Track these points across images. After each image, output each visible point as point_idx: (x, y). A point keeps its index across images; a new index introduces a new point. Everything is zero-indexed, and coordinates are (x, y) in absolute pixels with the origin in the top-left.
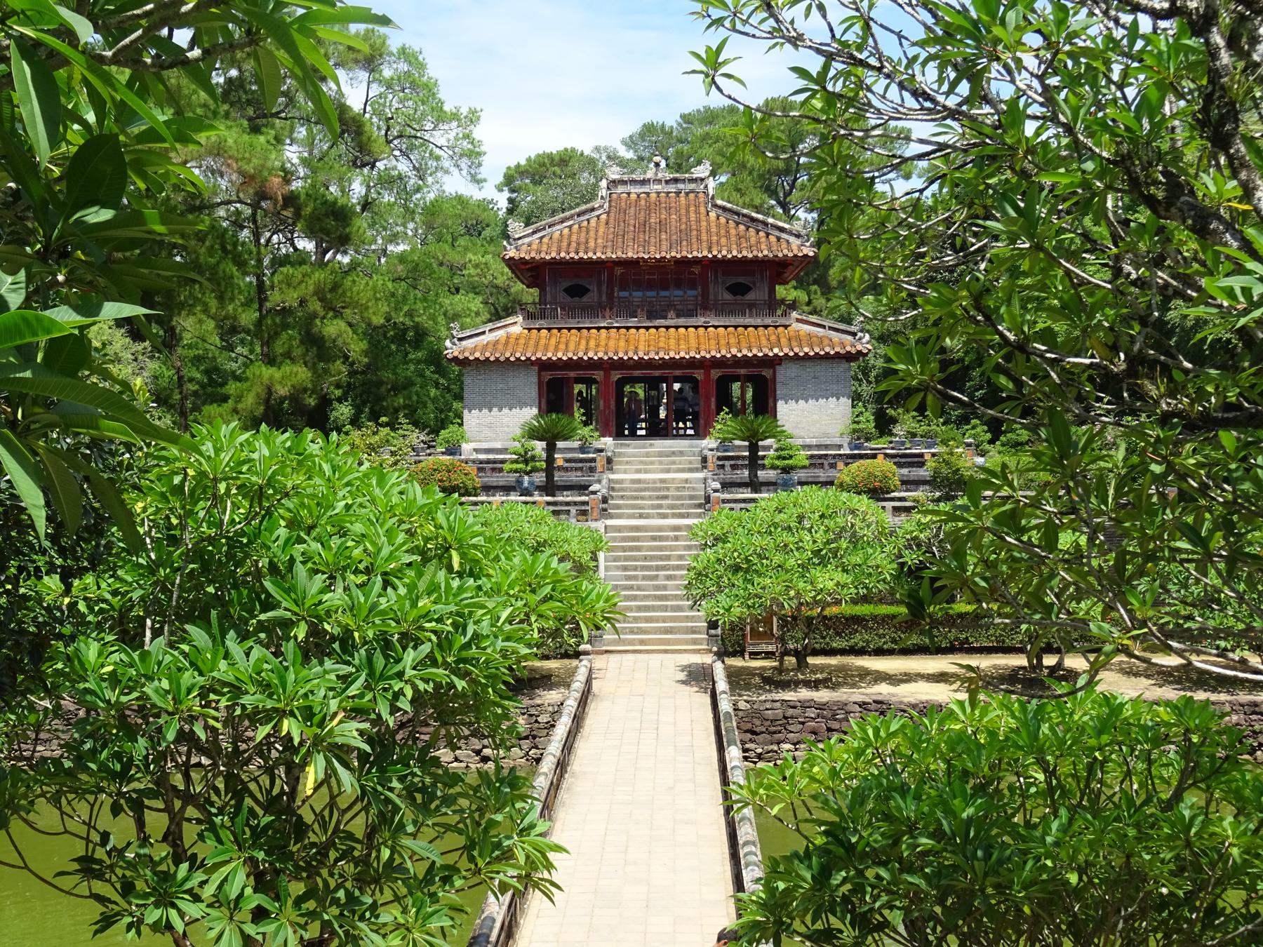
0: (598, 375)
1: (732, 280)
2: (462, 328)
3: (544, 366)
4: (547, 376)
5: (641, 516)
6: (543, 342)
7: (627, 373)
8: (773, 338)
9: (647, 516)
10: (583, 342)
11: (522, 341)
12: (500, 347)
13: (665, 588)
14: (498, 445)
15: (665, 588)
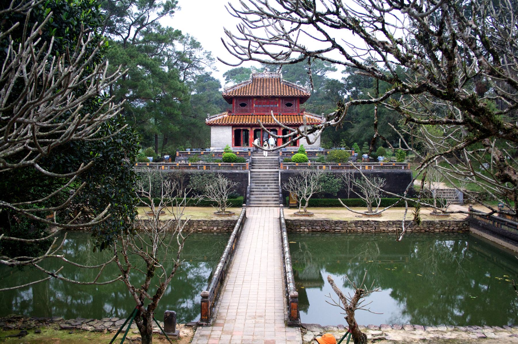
0: (249, 129)
1: (287, 102)
2: (211, 115)
3: (233, 126)
4: (234, 129)
5: (260, 169)
6: (233, 119)
7: (257, 128)
8: (298, 119)
9: (261, 169)
10: (245, 119)
11: (227, 119)
12: (221, 120)
13: (267, 188)
14: (221, 148)
15: (267, 188)
